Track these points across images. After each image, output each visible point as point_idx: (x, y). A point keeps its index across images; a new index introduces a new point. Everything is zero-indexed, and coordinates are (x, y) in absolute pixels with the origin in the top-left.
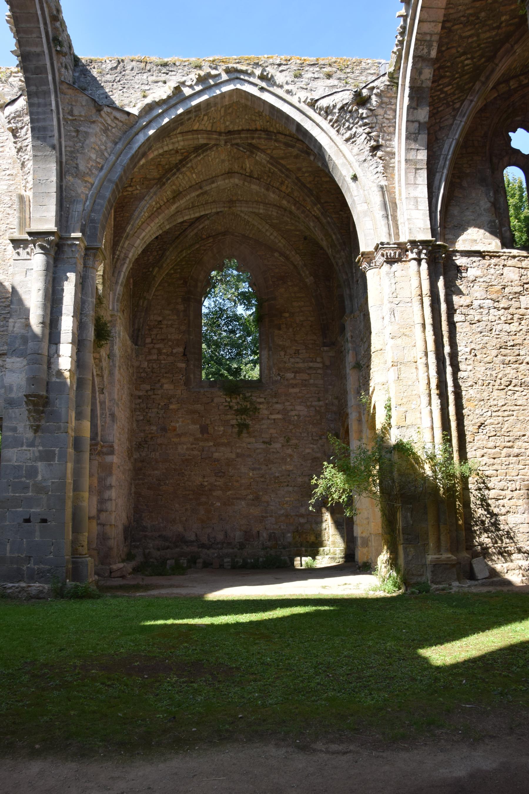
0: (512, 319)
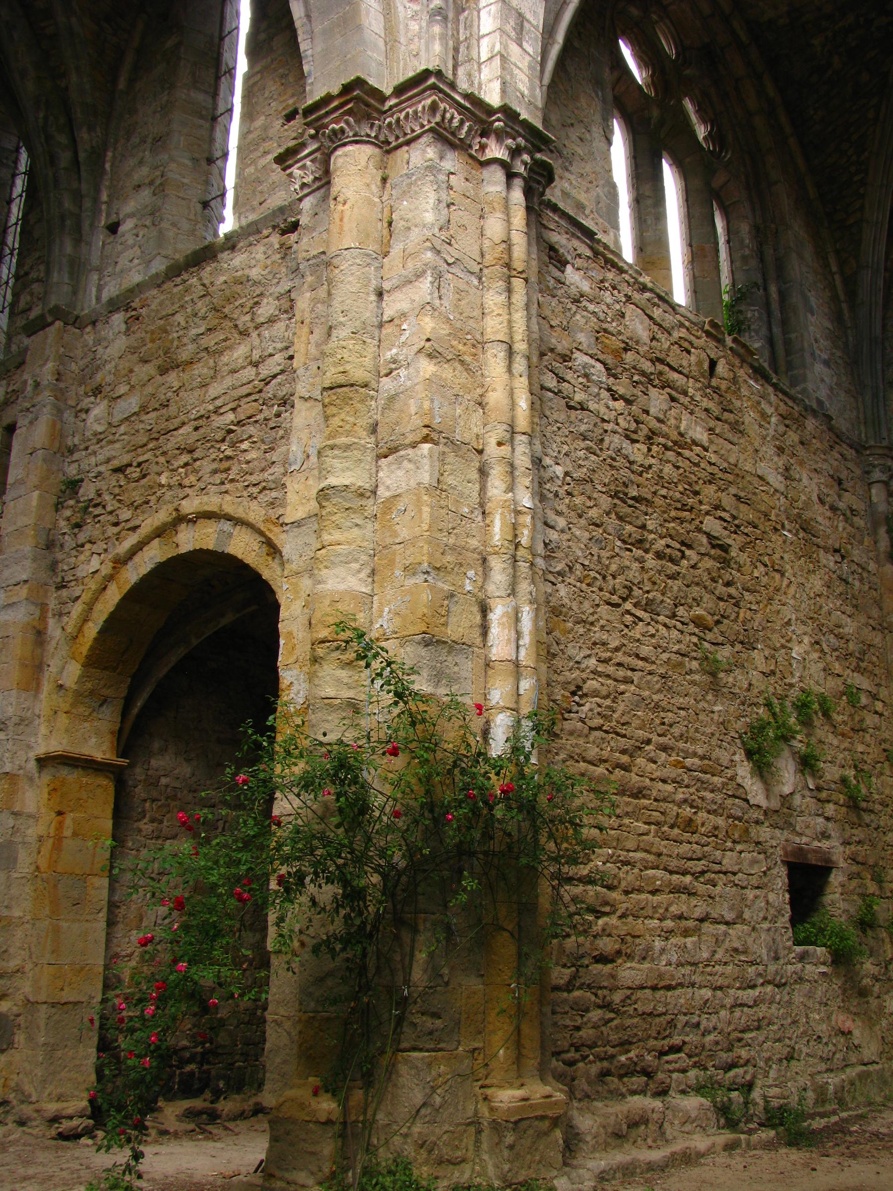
0: (635, 432)
